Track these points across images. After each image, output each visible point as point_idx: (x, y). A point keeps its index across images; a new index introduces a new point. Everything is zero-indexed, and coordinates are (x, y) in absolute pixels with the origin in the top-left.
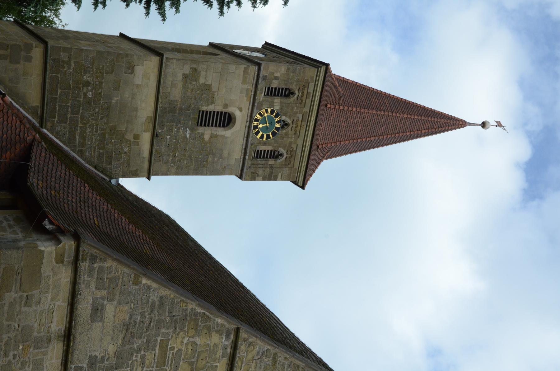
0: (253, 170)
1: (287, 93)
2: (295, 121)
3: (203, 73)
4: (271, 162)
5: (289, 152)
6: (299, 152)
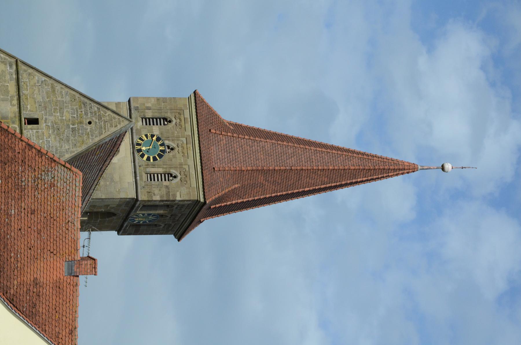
5: (182, 173)
6: (193, 172)
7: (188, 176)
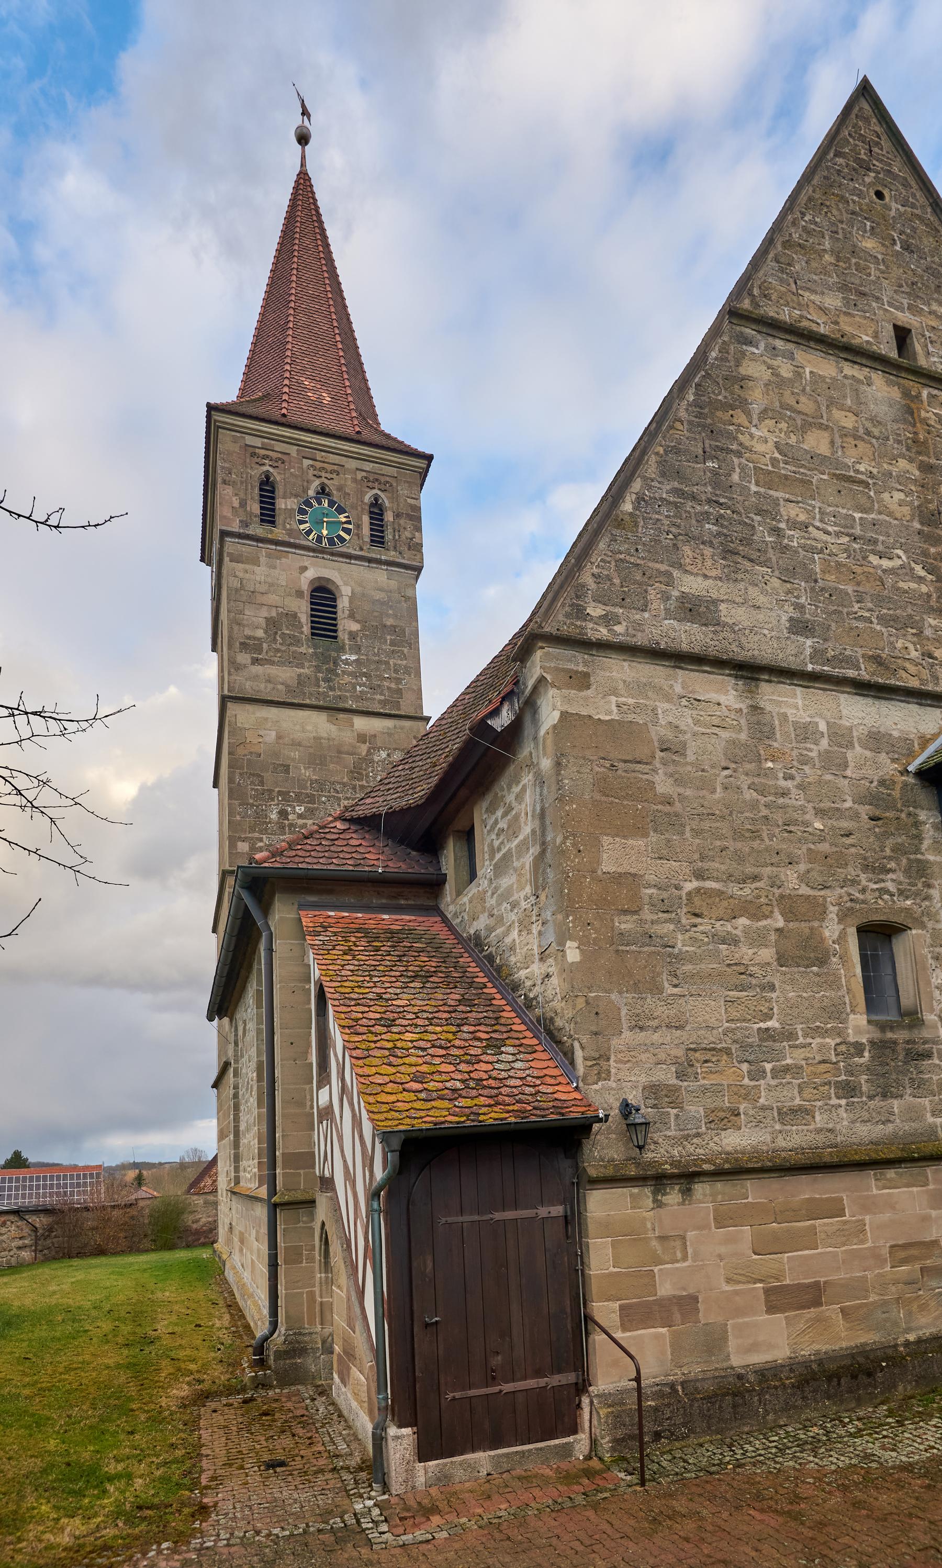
0: (404, 548)
1: (267, 489)
2: (315, 473)
3: (248, 632)
4: (389, 517)
5: (370, 484)
6: (368, 466)
7: (376, 476)
